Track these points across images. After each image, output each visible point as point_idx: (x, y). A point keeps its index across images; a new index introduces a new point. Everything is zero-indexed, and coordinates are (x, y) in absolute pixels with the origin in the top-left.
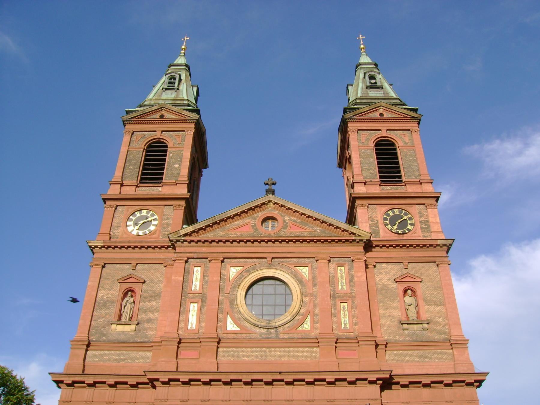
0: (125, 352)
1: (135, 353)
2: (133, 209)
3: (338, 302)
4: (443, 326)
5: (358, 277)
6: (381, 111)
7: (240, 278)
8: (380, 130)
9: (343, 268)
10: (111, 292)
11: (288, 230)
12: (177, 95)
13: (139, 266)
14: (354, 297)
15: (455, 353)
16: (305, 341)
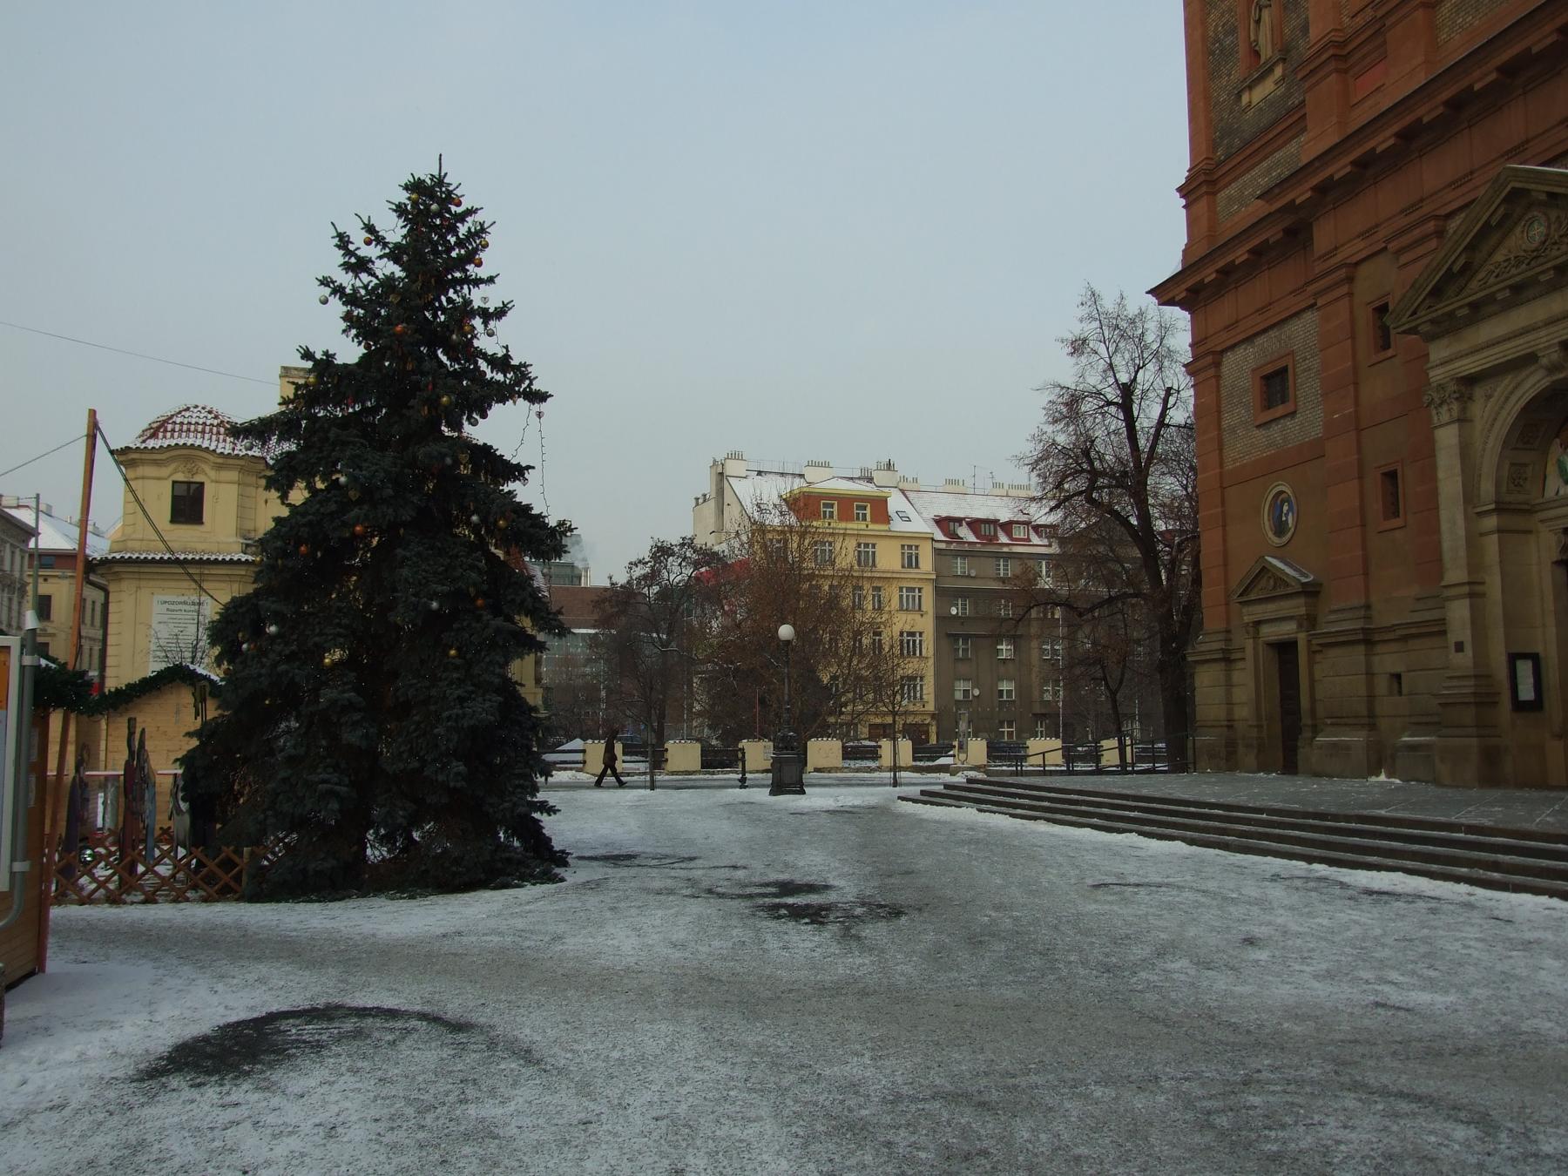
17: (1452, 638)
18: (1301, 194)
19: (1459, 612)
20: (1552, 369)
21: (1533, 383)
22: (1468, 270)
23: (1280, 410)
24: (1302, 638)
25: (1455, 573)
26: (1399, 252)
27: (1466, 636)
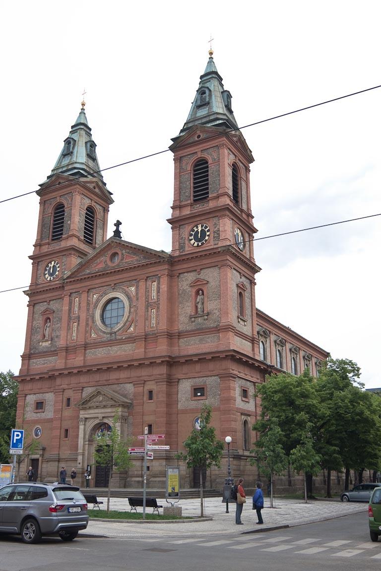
0: (47, 358)
1: (51, 358)
2: (46, 263)
3: (150, 309)
4: (218, 316)
5: (162, 289)
6: (198, 132)
7: (98, 301)
8: (196, 152)
9: (155, 283)
10: (38, 322)
11: (124, 261)
12: (71, 159)
13: (51, 302)
14: (159, 304)
15: (221, 336)
16: (132, 339)
17: (78, 462)
18: (57, 373)
19: (80, 458)
20: (100, 420)
21: (97, 421)
22: (89, 401)
23: (40, 410)
24: (40, 459)
25: (80, 451)
26: (74, 390)
27: (81, 462)
